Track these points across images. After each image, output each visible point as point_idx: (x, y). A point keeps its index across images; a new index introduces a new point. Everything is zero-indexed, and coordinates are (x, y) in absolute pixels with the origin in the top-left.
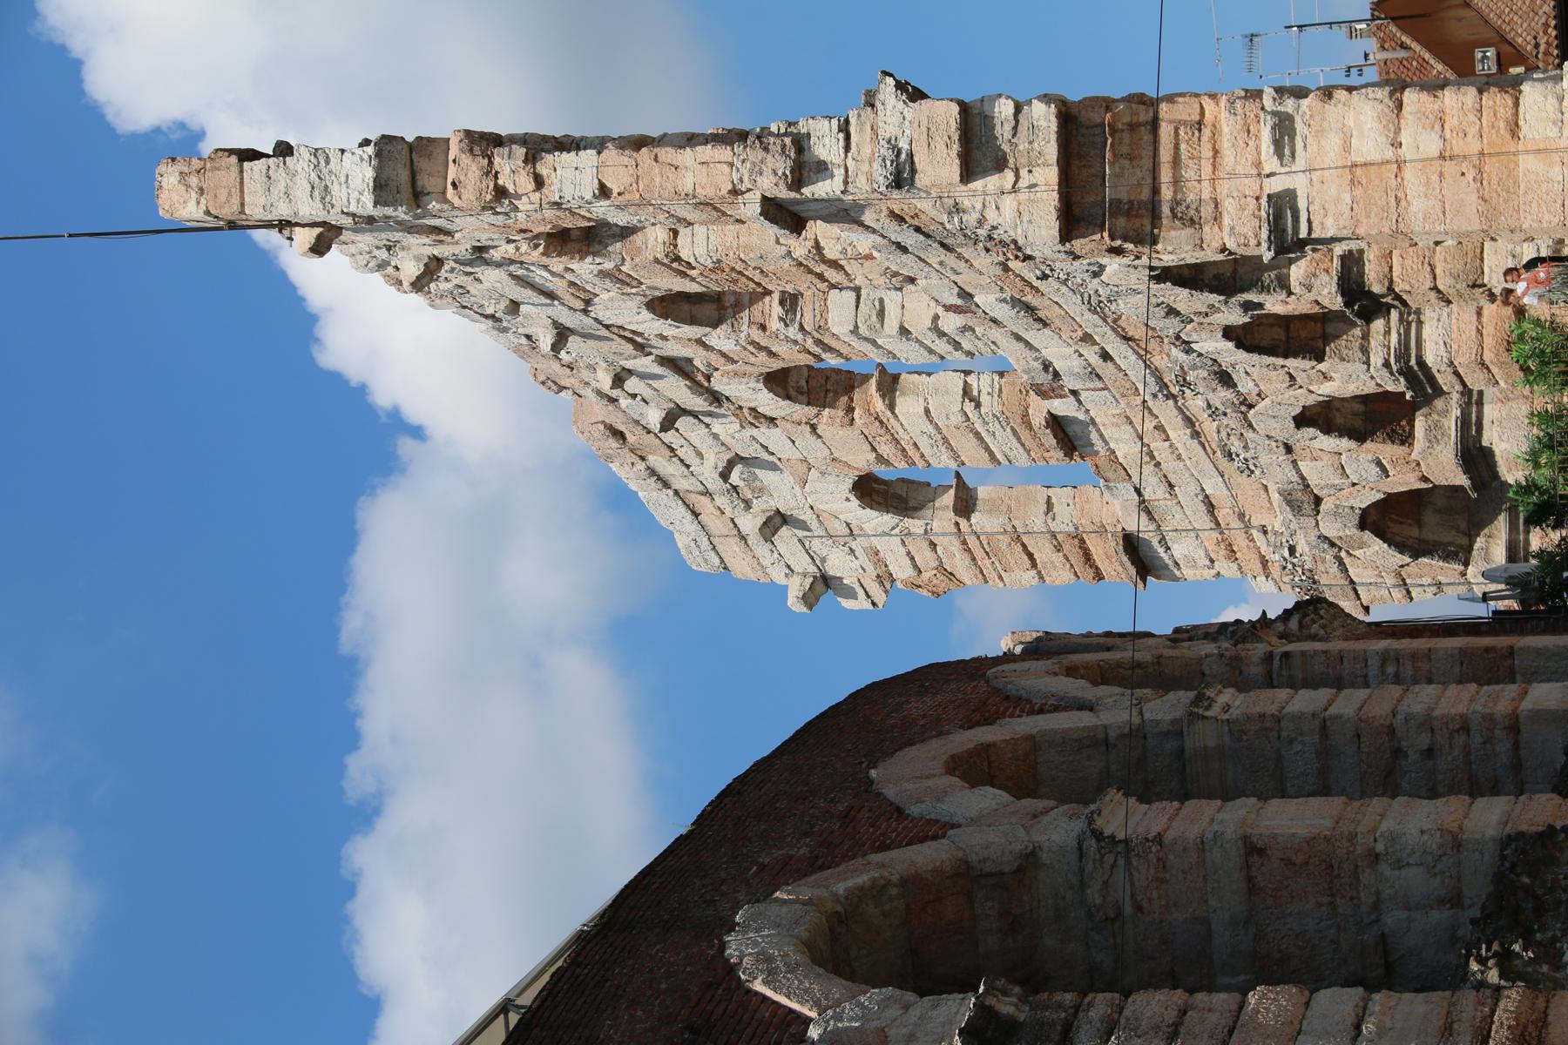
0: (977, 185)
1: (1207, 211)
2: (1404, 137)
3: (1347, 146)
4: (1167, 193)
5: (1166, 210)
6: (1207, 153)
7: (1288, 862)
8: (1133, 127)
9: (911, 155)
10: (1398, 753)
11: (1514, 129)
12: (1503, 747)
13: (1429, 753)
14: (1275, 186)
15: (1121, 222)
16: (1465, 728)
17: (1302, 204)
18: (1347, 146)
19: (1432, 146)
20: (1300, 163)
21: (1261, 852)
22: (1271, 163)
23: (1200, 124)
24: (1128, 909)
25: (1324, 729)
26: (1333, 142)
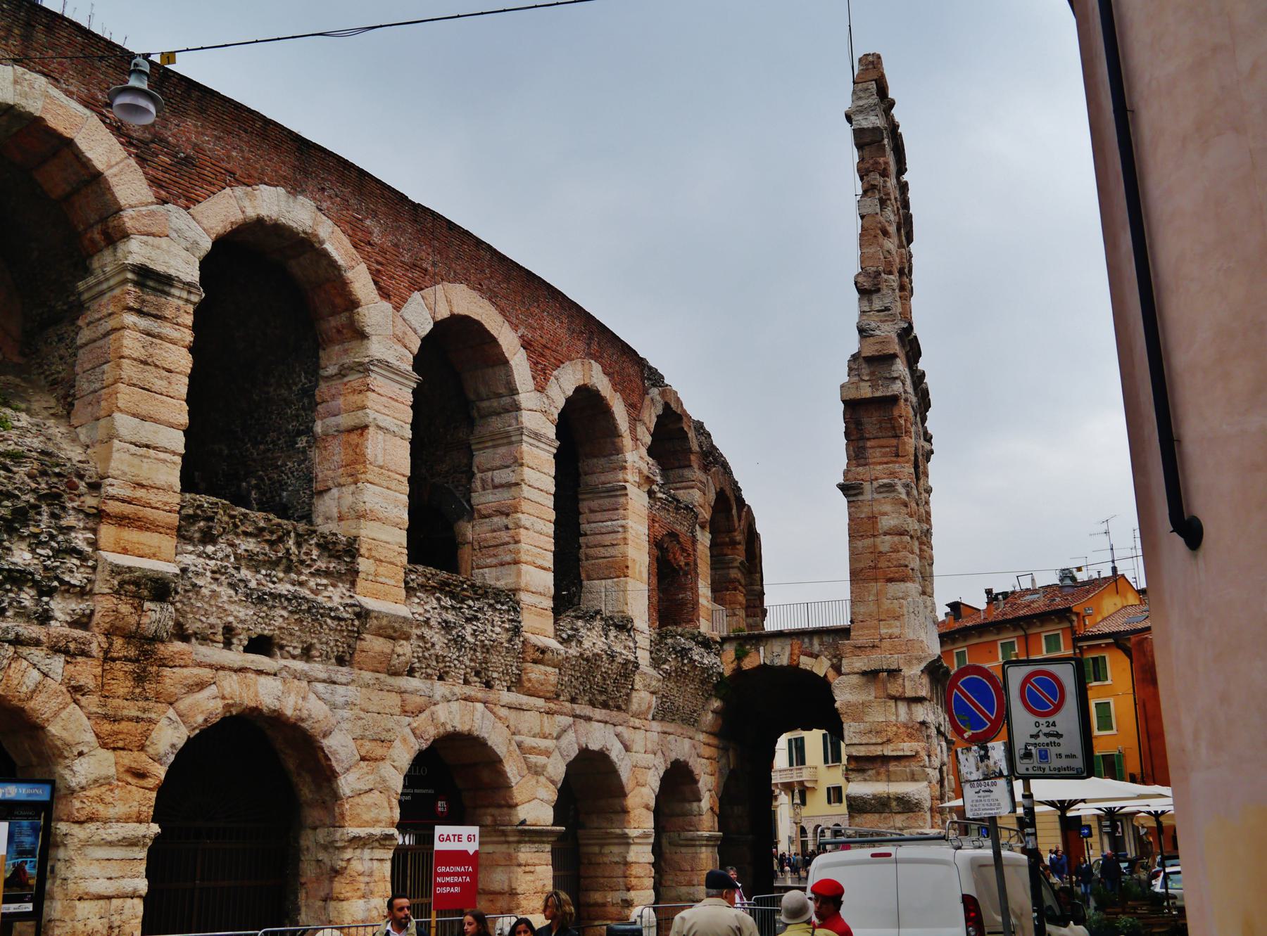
0: (864, 365)
1: (862, 461)
2: (888, 537)
3: (885, 514)
4: (869, 444)
5: (861, 444)
6: (885, 460)
7: (357, 446)
8: (894, 428)
9: (872, 336)
10: (507, 515)
11: (890, 580)
12: (508, 558)
13: (507, 528)
14: (867, 486)
15: (853, 426)
16: (517, 542)
17: (860, 498)
18: (885, 514)
19: (884, 548)
20: (876, 496)
21: (362, 434)
22: (875, 484)
23: (897, 456)
24: (346, 380)
25: (517, 484)
26: (887, 508)
